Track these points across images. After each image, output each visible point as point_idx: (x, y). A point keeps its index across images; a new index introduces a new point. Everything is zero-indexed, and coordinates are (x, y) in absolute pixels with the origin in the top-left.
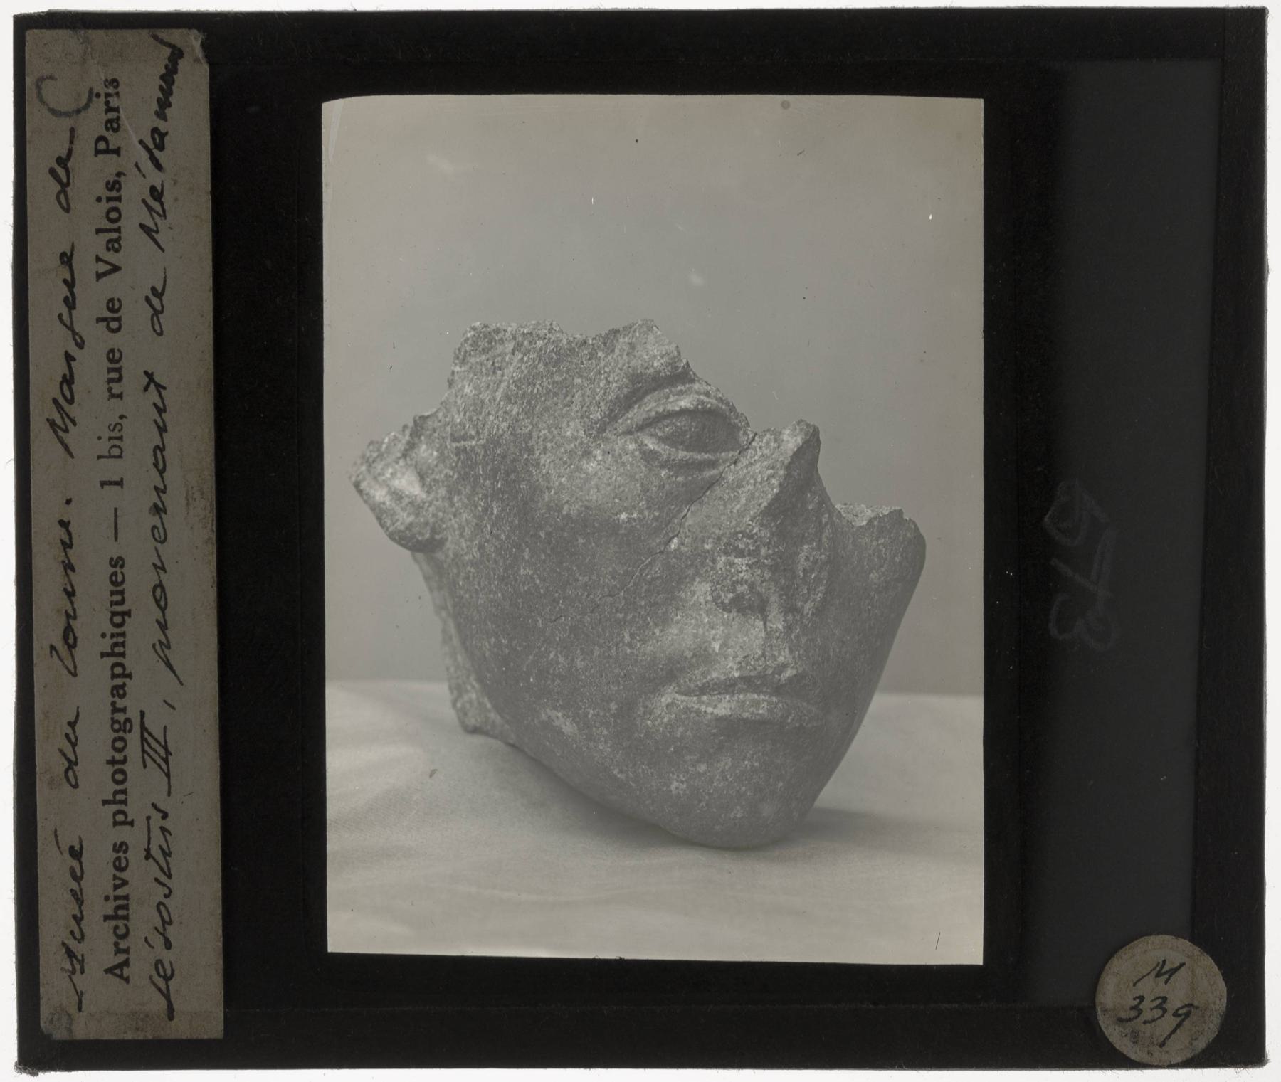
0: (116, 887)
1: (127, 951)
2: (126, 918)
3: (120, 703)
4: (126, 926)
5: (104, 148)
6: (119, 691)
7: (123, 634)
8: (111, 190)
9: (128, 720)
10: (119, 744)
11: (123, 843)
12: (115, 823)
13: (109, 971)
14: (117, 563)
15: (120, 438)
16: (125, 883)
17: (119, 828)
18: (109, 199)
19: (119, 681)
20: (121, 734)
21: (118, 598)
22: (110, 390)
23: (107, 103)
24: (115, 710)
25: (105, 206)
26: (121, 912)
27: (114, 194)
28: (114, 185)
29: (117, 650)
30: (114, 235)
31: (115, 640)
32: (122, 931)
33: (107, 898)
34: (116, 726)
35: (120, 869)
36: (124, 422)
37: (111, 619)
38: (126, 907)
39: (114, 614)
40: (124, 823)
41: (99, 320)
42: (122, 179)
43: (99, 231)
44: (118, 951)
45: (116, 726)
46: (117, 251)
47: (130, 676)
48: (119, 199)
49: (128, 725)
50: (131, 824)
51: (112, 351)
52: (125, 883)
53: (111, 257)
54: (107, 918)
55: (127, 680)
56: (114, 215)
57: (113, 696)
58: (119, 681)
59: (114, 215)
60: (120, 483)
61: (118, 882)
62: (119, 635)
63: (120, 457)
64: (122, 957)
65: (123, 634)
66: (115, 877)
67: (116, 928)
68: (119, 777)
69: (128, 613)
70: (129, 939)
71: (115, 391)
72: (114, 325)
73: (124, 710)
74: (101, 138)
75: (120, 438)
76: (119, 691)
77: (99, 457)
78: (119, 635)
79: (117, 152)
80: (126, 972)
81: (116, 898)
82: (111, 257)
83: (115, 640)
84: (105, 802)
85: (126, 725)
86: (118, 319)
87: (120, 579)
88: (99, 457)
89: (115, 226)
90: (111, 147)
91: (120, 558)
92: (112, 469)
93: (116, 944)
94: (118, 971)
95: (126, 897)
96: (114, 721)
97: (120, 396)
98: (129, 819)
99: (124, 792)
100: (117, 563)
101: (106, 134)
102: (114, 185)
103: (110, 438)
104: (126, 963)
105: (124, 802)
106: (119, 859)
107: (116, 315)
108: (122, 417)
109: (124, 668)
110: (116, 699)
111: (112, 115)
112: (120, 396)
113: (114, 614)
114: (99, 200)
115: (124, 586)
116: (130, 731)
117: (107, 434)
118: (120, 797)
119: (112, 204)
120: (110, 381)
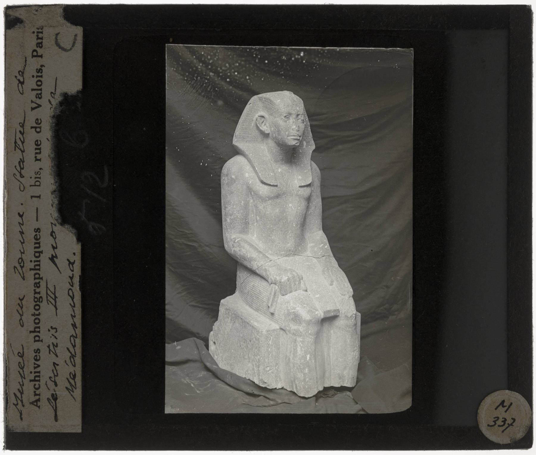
0: (35, 368)
1: (39, 395)
2: (39, 381)
3: (38, 290)
4: (39, 384)
5: (36, 55)
6: (37, 285)
7: (39, 261)
8: (38, 72)
9: (41, 297)
10: (37, 307)
11: (38, 349)
12: (35, 341)
13: (32, 403)
14: (38, 230)
15: (40, 178)
16: (39, 366)
17: (36, 343)
18: (37, 76)
19: (37, 281)
20: (38, 303)
21: (37, 245)
22: (36, 157)
23: (37, 36)
24: (36, 293)
25: (36, 79)
26: (37, 379)
27: (40, 74)
28: (39, 71)
29: (37, 267)
30: (39, 92)
31: (36, 263)
32: (37, 386)
33: (31, 372)
34: (36, 300)
35: (36, 360)
36: (41, 171)
37: (34, 255)
38: (39, 376)
39: (36, 252)
40: (38, 341)
41: (32, 128)
42: (43, 68)
43: (33, 90)
44: (36, 395)
45: (36, 300)
46: (40, 98)
47: (42, 278)
48: (41, 76)
49: (41, 300)
50: (42, 341)
51: (37, 141)
52: (39, 366)
53: (38, 101)
54: (31, 381)
55: (41, 280)
56: (39, 83)
57: (35, 287)
58: (37, 281)
59: (39, 83)
60: (39, 197)
61: (36, 366)
62: (37, 261)
63: (39, 186)
64: (37, 397)
65: (39, 261)
66: (35, 364)
67: (35, 385)
68: (37, 321)
69: (42, 252)
70: (40, 389)
71: (38, 158)
72: (38, 130)
73: (39, 293)
74: (34, 51)
75: (40, 178)
76: (37, 285)
77: (31, 186)
78: (37, 261)
79: (41, 56)
80: (39, 404)
81: (35, 372)
82: (38, 101)
83: (36, 263)
84: (31, 332)
85: (40, 299)
86: (40, 128)
87: (38, 238)
88: (31, 186)
89: (40, 88)
90: (39, 54)
91: (38, 229)
92: (36, 191)
93: (35, 392)
94: (35, 404)
95: (39, 372)
96: (35, 298)
97: (40, 160)
98: (41, 339)
99: (39, 327)
100: (38, 230)
101: (35, 48)
102: (39, 71)
103: (36, 178)
104: (39, 400)
105: (39, 332)
106: (36, 356)
107: (39, 126)
108: (40, 169)
109: (39, 274)
110: (36, 288)
111: (40, 41)
112: (40, 160)
113: (36, 252)
114: (33, 76)
115: (40, 240)
116: (42, 302)
117: (34, 176)
118: (37, 330)
119: (38, 79)
120: (36, 153)
